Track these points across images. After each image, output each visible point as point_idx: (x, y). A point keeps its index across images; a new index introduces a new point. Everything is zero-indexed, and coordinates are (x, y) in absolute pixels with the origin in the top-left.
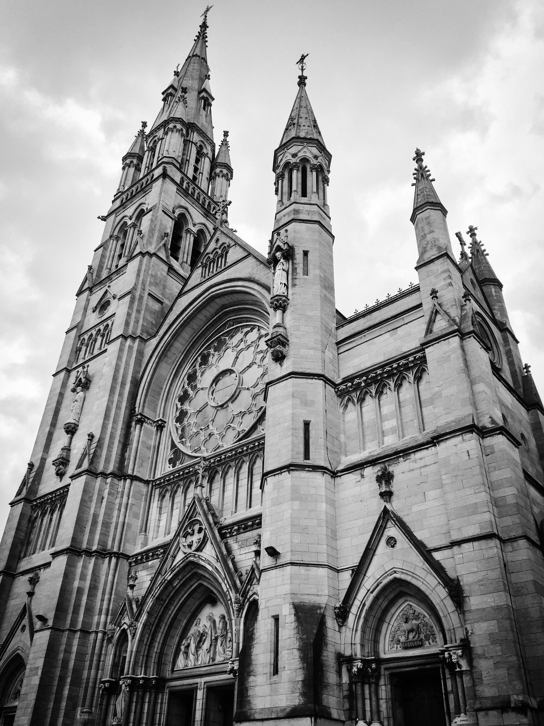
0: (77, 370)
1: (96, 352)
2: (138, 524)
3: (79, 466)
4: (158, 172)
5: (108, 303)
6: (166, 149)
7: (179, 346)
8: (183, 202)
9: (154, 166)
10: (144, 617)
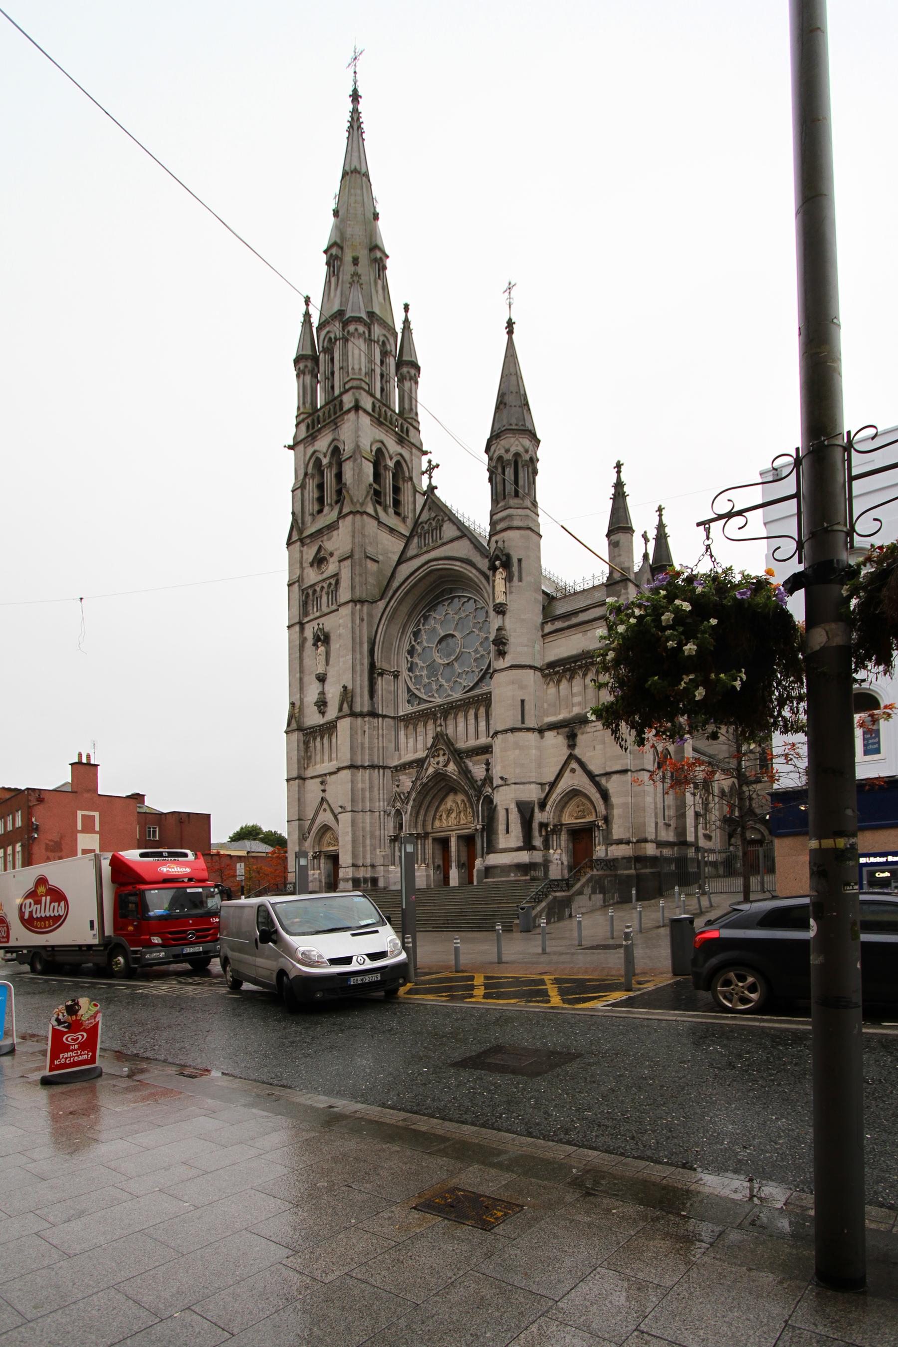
2: (393, 745)
7: (404, 609)
8: (379, 434)
10: (411, 803)
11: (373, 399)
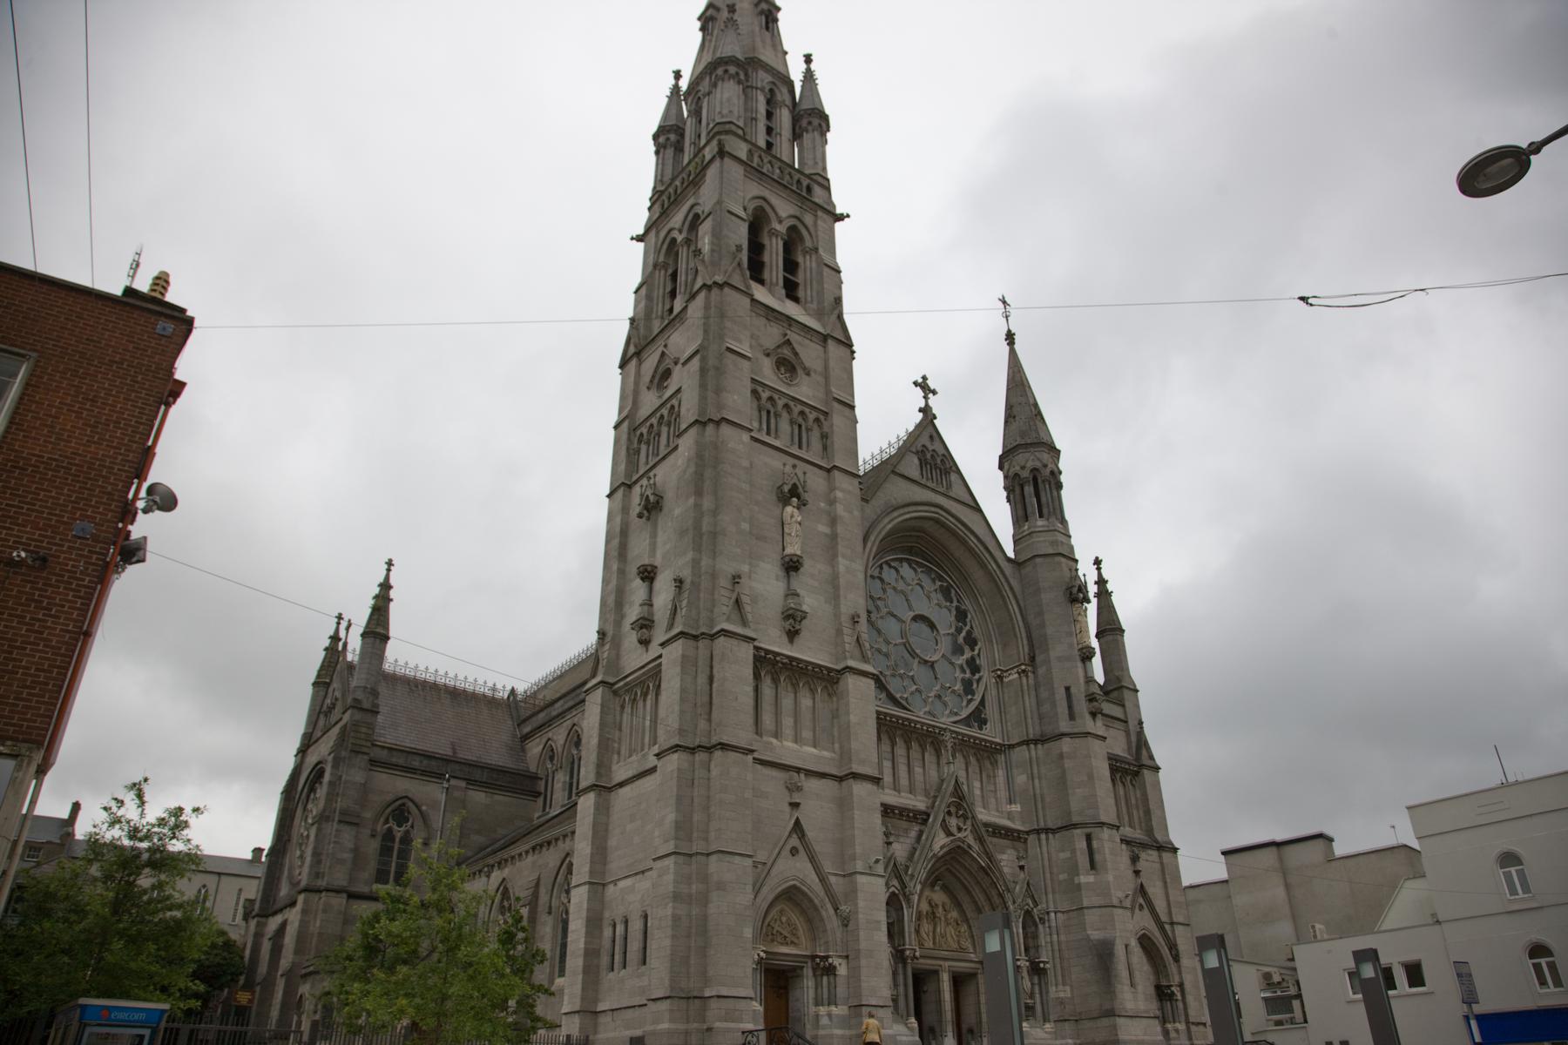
0: (639, 484)
1: (663, 452)
3: (671, 626)
4: (708, 153)
5: (667, 374)
6: (718, 110)
8: (755, 189)
9: (703, 142)
11: (750, 146)
